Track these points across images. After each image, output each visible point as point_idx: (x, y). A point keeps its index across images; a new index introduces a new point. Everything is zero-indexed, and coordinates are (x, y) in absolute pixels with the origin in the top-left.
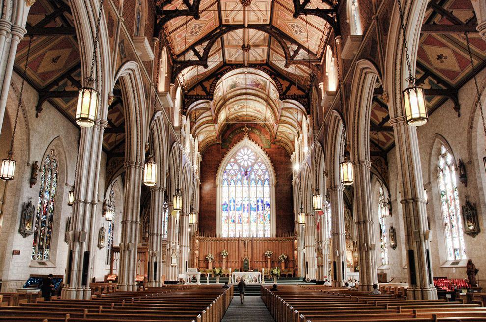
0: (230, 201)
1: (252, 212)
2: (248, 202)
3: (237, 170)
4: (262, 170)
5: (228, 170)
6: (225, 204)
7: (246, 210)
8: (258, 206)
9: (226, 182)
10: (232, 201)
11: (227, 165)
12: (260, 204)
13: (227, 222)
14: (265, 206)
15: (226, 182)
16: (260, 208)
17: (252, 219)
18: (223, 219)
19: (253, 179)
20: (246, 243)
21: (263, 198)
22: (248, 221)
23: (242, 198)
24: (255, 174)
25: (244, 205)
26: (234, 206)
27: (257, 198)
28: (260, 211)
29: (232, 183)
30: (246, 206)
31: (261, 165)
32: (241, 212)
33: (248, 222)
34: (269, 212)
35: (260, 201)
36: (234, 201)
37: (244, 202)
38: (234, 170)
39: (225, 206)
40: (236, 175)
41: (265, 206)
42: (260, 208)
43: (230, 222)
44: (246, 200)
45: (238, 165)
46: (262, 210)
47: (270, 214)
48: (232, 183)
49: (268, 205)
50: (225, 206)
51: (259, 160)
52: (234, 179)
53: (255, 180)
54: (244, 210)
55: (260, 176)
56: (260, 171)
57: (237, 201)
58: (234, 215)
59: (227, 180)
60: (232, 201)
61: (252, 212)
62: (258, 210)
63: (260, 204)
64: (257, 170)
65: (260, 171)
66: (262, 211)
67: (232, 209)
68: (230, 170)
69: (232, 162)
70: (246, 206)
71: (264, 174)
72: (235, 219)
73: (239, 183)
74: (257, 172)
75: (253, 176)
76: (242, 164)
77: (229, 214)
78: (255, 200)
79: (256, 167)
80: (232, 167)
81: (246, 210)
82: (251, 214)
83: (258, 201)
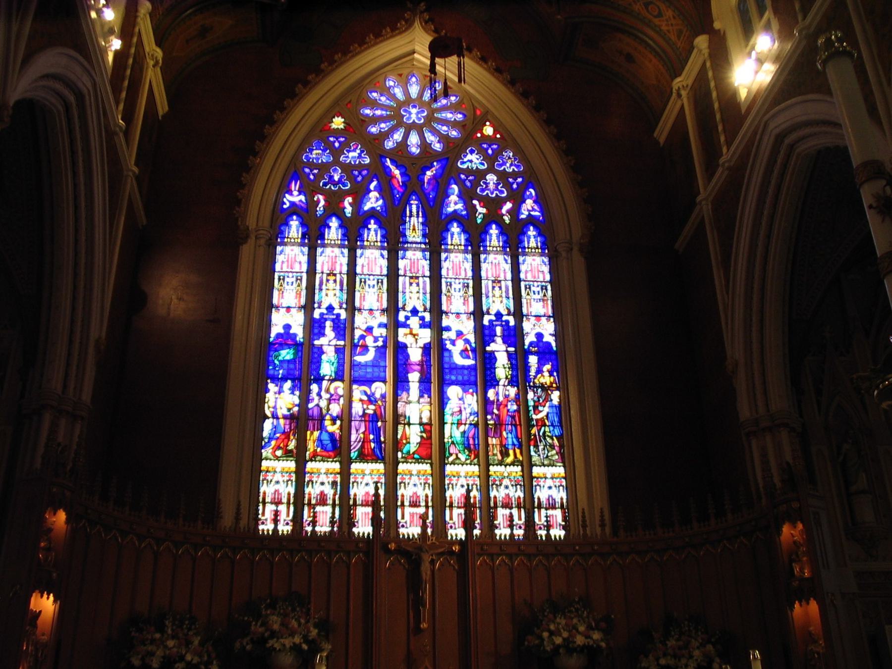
0: (321, 323)
1: (453, 392)
2: (426, 336)
3: (361, 167)
4: (503, 177)
5: (312, 166)
6: (286, 339)
7: (414, 377)
8: (489, 360)
9: (294, 229)
10: (328, 324)
11: (305, 145)
12: (498, 347)
13: (292, 445)
14: (533, 360)
15: (294, 229)
16: (502, 371)
17: (453, 433)
18: (268, 426)
19: (455, 217)
20: (426, 568)
21: (518, 313)
22: (425, 442)
23: (393, 307)
24: (466, 196)
25: (401, 349)
26: (339, 351)
27: (478, 313)
28: (504, 391)
29: (334, 232)
30: (415, 355)
31: (498, 153)
32: (379, 389)
33: (424, 453)
34: (555, 396)
35: (499, 330)
36: (343, 329)
37: (403, 335)
38: (348, 169)
39: (287, 354)
40: (360, 195)
41: (533, 360)
42: (502, 371)
43: (311, 446)
44: (414, 322)
45: (374, 145)
46: (512, 382)
47: (561, 409)
48: (334, 232)
49: (544, 351)
50: (287, 354)
51: (488, 130)
52: (348, 210)
53: (466, 221)
54: (400, 383)
55: (493, 205)
56: (491, 178)
57: (361, 321)
58: (335, 409)
59: (304, 213)
60: (328, 324)
61: (453, 392)
62: (491, 381)
63: (498, 347)
64: (479, 175)
65: (491, 178)
66: (512, 391)
67: (327, 368)
68: (324, 168)
69: (337, 133)
70: (415, 355)
71: (518, 199)
72: (346, 429)
73: (373, 234)
74: (475, 184)
75: (454, 204)
76: (389, 144)
77: (305, 398)
78: (468, 326)
79: (473, 160)
80: (336, 153)
81: (414, 377)
82: (442, 401)
83: (484, 334)
